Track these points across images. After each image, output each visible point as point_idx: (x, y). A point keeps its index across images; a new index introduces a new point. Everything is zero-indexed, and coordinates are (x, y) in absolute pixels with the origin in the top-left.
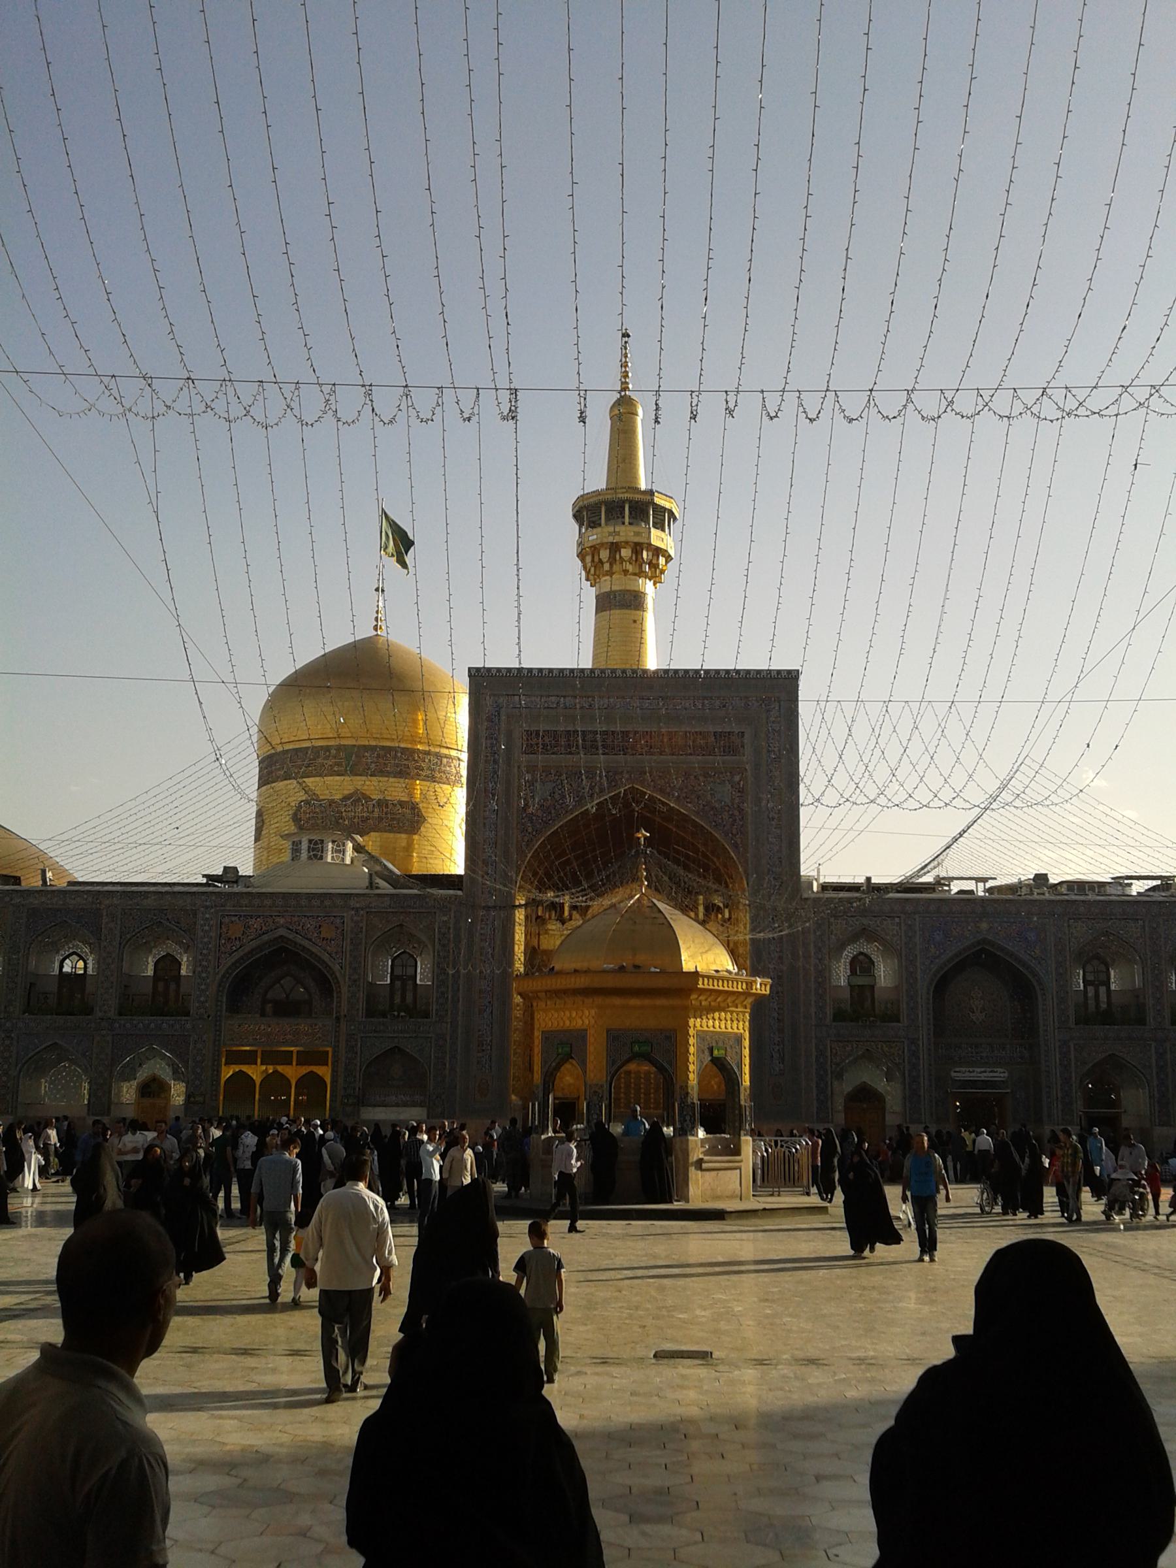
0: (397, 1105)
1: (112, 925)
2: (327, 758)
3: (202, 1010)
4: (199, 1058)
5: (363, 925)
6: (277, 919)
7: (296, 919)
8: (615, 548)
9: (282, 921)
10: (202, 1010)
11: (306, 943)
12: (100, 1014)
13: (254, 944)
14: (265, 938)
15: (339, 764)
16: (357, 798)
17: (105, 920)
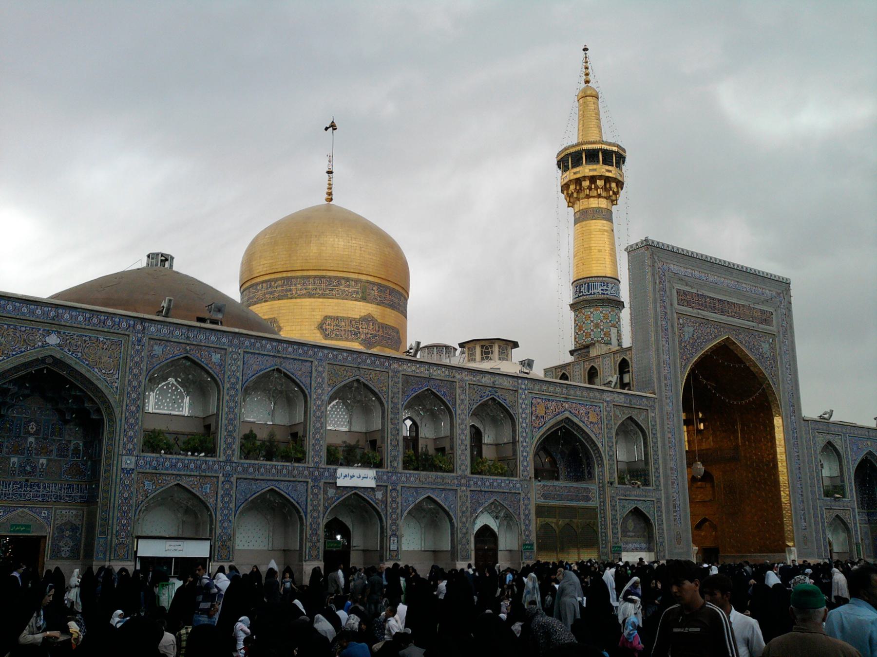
0: (633, 550)
1: (463, 397)
2: (349, 286)
3: (526, 473)
4: (527, 512)
5: (612, 414)
6: (564, 404)
7: (574, 405)
8: (593, 179)
9: (567, 406)
10: (526, 473)
11: (581, 424)
12: (459, 473)
13: (552, 422)
14: (559, 418)
15: (357, 293)
16: (368, 319)
17: (458, 391)
